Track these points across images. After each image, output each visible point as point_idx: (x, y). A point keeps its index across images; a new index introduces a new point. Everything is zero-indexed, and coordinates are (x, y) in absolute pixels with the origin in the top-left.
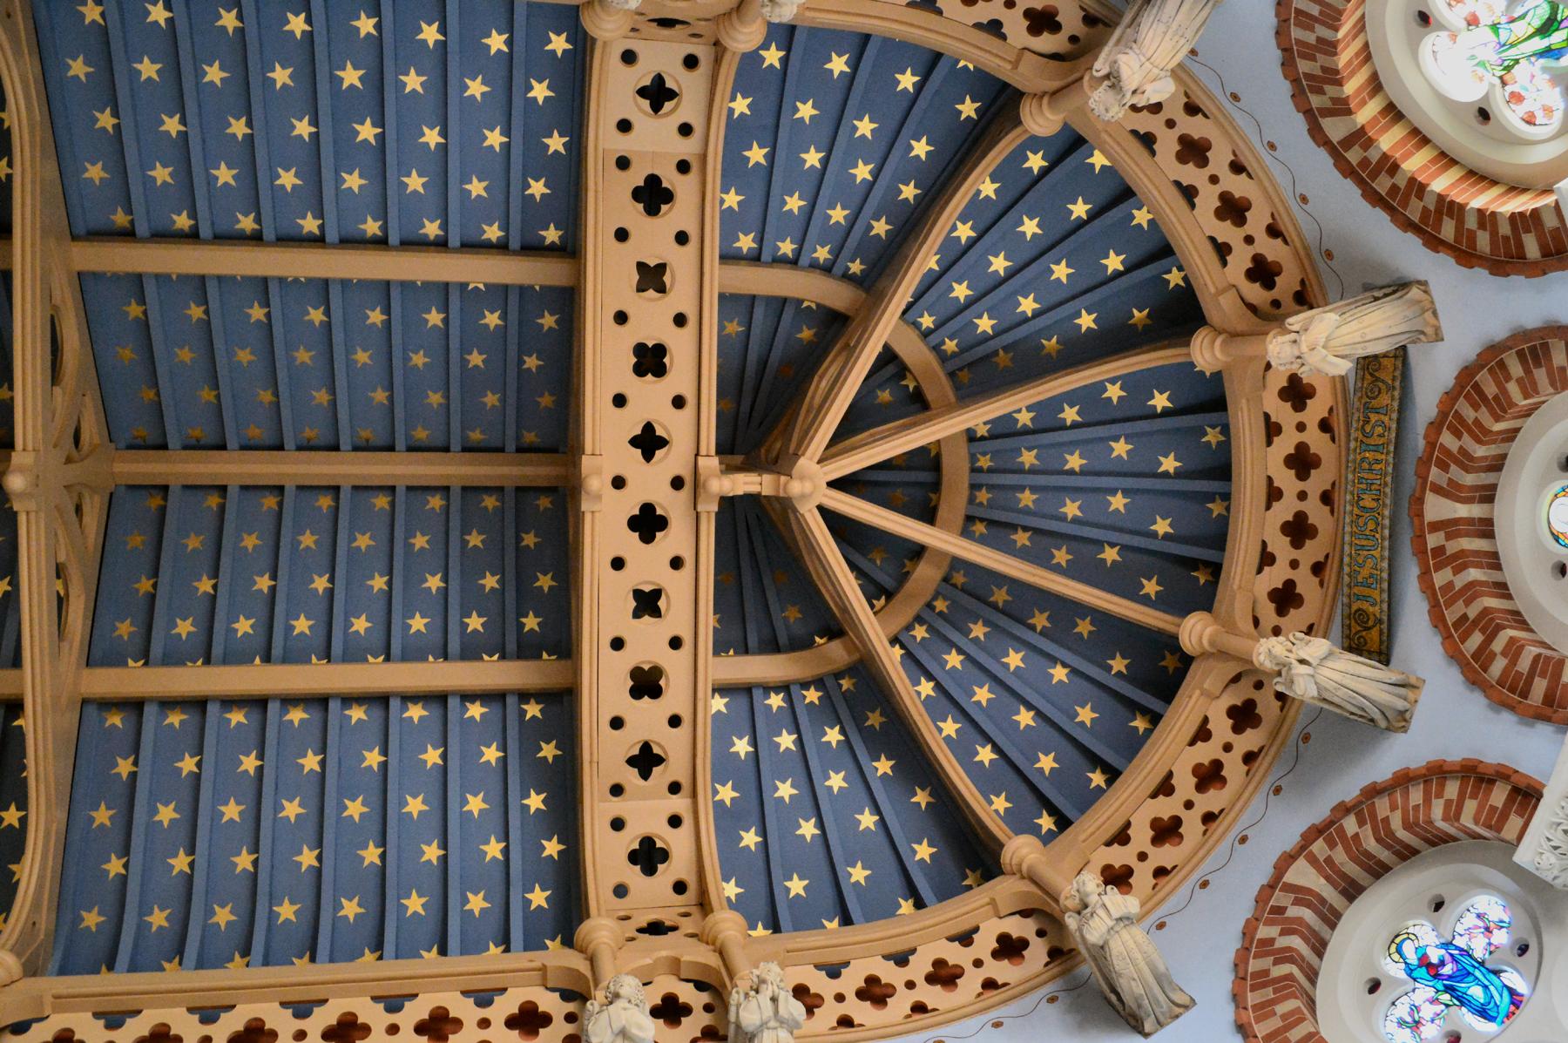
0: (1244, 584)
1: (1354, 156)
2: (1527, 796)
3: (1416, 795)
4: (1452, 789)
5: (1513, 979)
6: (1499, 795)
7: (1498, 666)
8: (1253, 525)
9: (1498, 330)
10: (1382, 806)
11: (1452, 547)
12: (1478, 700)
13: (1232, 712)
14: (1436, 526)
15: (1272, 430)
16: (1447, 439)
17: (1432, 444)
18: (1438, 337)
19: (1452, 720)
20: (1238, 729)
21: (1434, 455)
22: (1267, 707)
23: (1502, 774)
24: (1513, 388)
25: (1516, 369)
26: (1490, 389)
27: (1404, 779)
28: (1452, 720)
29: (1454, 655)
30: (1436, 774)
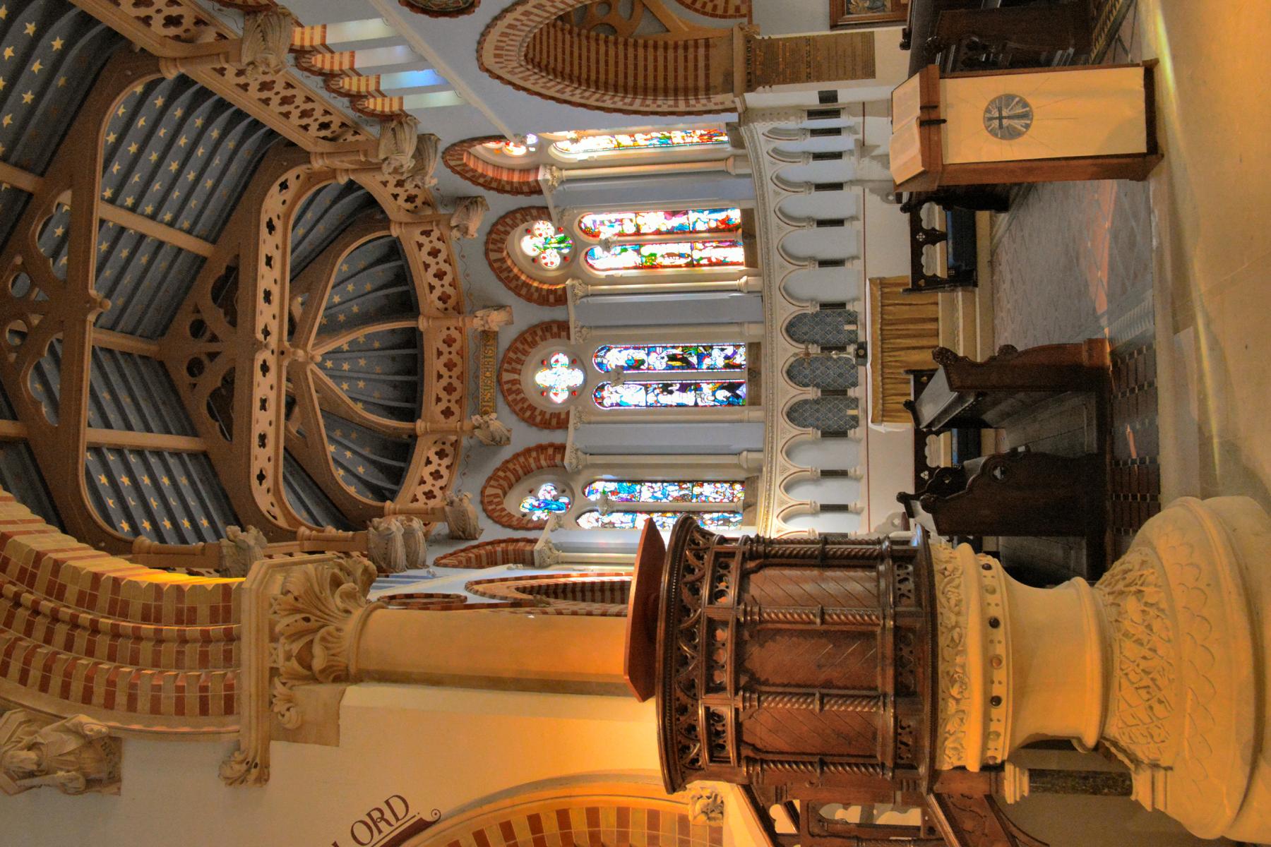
0: (432, 408)
1: (496, 265)
2: (561, 449)
3: (522, 459)
4: (534, 454)
5: (565, 500)
6: (550, 451)
7: (538, 419)
8: (433, 388)
9: (535, 321)
10: (511, 466)
11: (514, 388)
12: (534, 429)
13: (437, 453)
14: (508, 382)
15: (440, 353)
16: (512, 355)
17: (505, 356)
18: (512, 323)
19: (524, 437)
20: (441, 458)
21: (507, 360)
22: (449, 449)
23: (551, 445)
24: (538, 339)
25: (539, 333)
26: (529, 339)
27: (517, 456)
28: (524, 437)
29: (524, 420)
30: (528, 451)
